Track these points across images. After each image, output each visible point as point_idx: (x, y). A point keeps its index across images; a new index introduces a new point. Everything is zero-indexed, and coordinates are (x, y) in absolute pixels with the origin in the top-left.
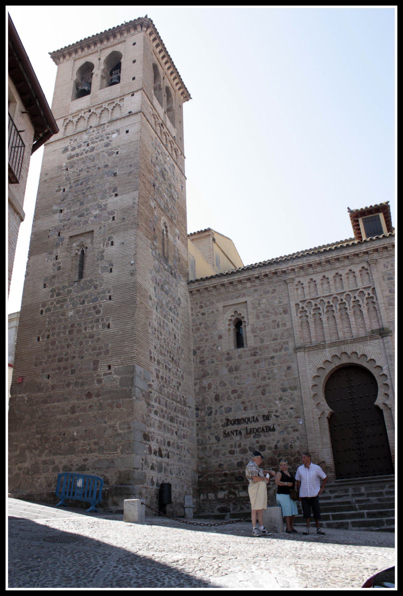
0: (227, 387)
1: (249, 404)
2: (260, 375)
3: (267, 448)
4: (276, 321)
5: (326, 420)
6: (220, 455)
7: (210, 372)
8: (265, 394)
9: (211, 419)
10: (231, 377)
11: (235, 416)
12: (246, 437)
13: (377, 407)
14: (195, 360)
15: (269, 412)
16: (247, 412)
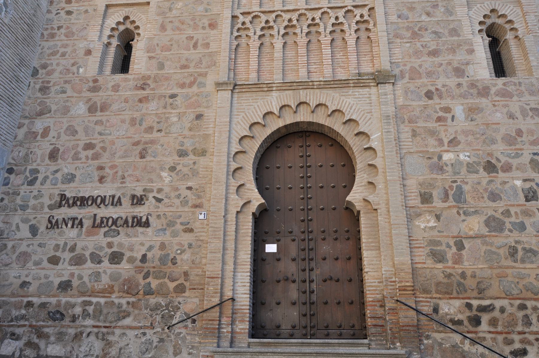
0: (77, 137)
1: (111, 172)
2: (144, 123)
3: (125, 258)
4: (193, 37)
5: (250, 218)
6: (30, 265)
7: (54, 108)
8: (144, 158)
9: (31, 192)
10: (89, 121)
11: (79, 191)
12: (89, 234)
13: (349, 209)
14: (32, 84)
15: (144, 190)
16: (105, 185)
